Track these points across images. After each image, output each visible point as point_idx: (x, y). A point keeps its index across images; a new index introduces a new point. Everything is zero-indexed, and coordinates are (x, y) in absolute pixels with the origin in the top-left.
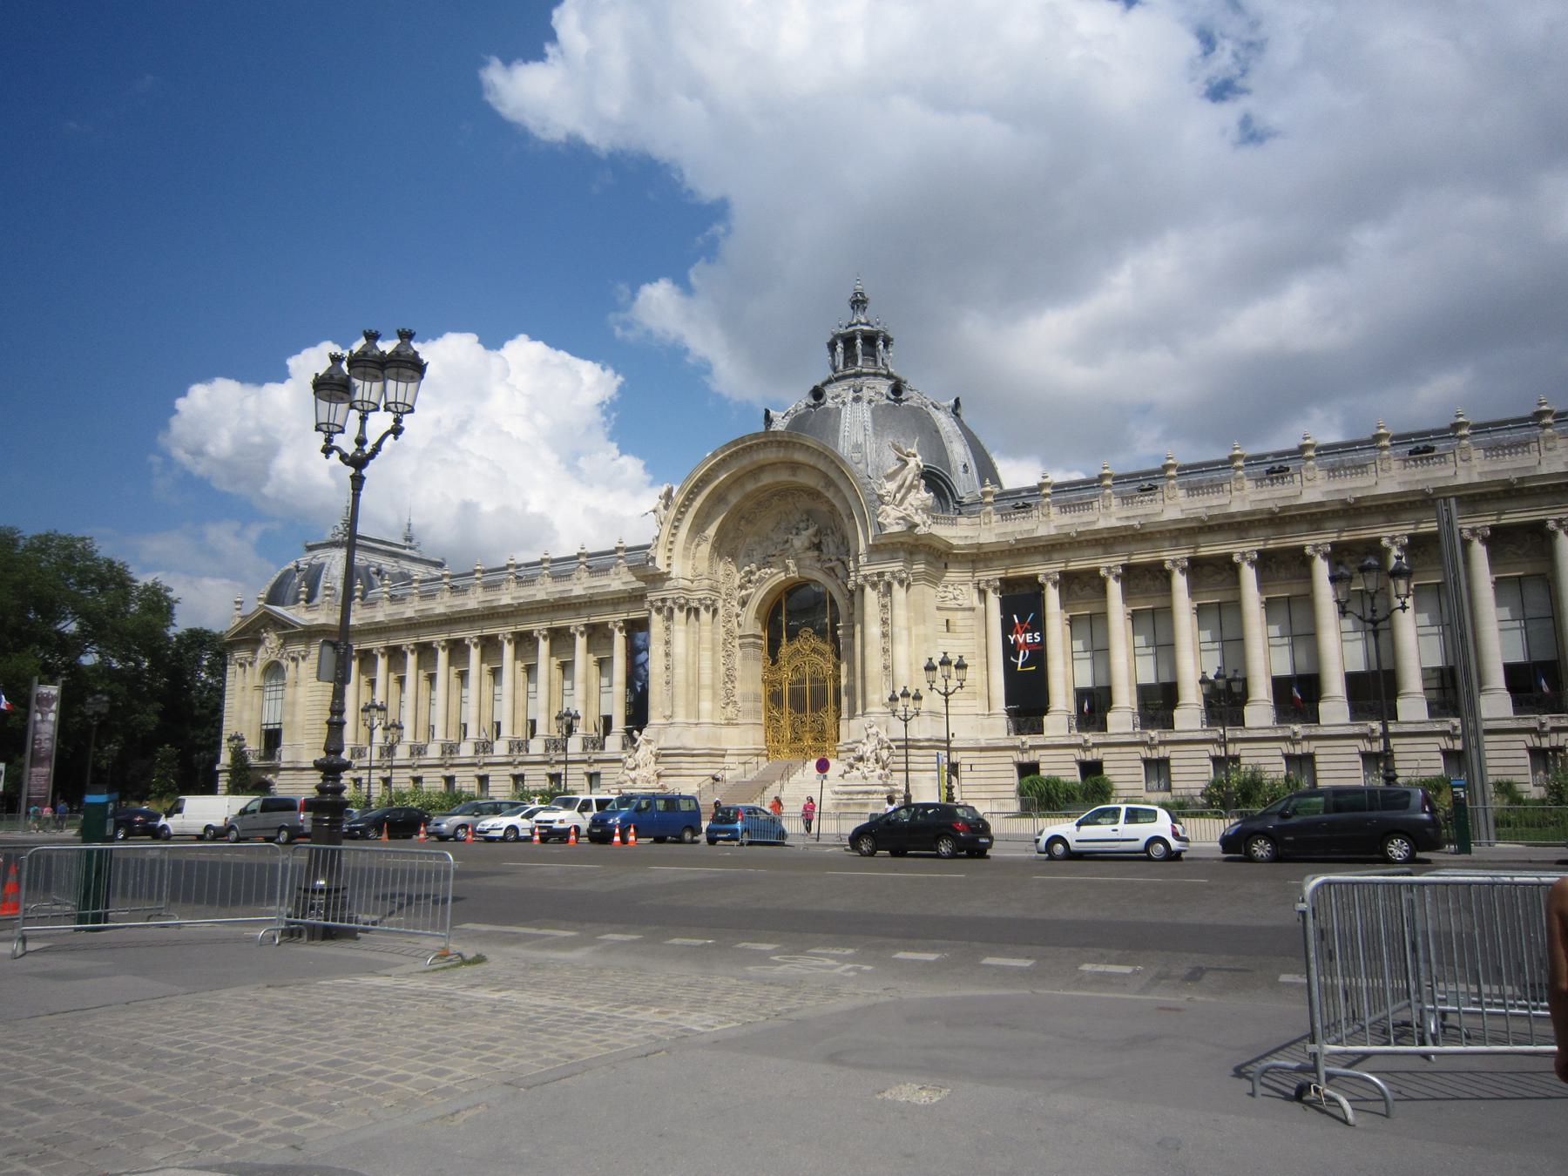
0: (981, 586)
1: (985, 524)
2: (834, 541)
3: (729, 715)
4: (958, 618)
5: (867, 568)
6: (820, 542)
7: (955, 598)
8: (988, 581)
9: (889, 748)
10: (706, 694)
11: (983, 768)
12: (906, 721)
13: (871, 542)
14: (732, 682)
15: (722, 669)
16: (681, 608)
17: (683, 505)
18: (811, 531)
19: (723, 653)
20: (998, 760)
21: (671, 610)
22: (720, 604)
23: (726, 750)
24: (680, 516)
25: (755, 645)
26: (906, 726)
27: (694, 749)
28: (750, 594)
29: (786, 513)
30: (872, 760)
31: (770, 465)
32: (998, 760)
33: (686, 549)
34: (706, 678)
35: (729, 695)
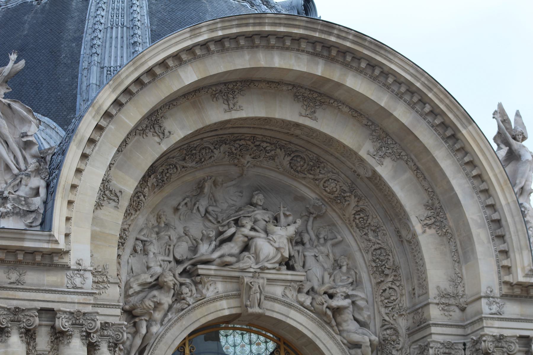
2: (316, 256)
5: (497, 324)
6: (293, 256)
13: (521, 279)
18: (291, 230)
31: (269, 82)
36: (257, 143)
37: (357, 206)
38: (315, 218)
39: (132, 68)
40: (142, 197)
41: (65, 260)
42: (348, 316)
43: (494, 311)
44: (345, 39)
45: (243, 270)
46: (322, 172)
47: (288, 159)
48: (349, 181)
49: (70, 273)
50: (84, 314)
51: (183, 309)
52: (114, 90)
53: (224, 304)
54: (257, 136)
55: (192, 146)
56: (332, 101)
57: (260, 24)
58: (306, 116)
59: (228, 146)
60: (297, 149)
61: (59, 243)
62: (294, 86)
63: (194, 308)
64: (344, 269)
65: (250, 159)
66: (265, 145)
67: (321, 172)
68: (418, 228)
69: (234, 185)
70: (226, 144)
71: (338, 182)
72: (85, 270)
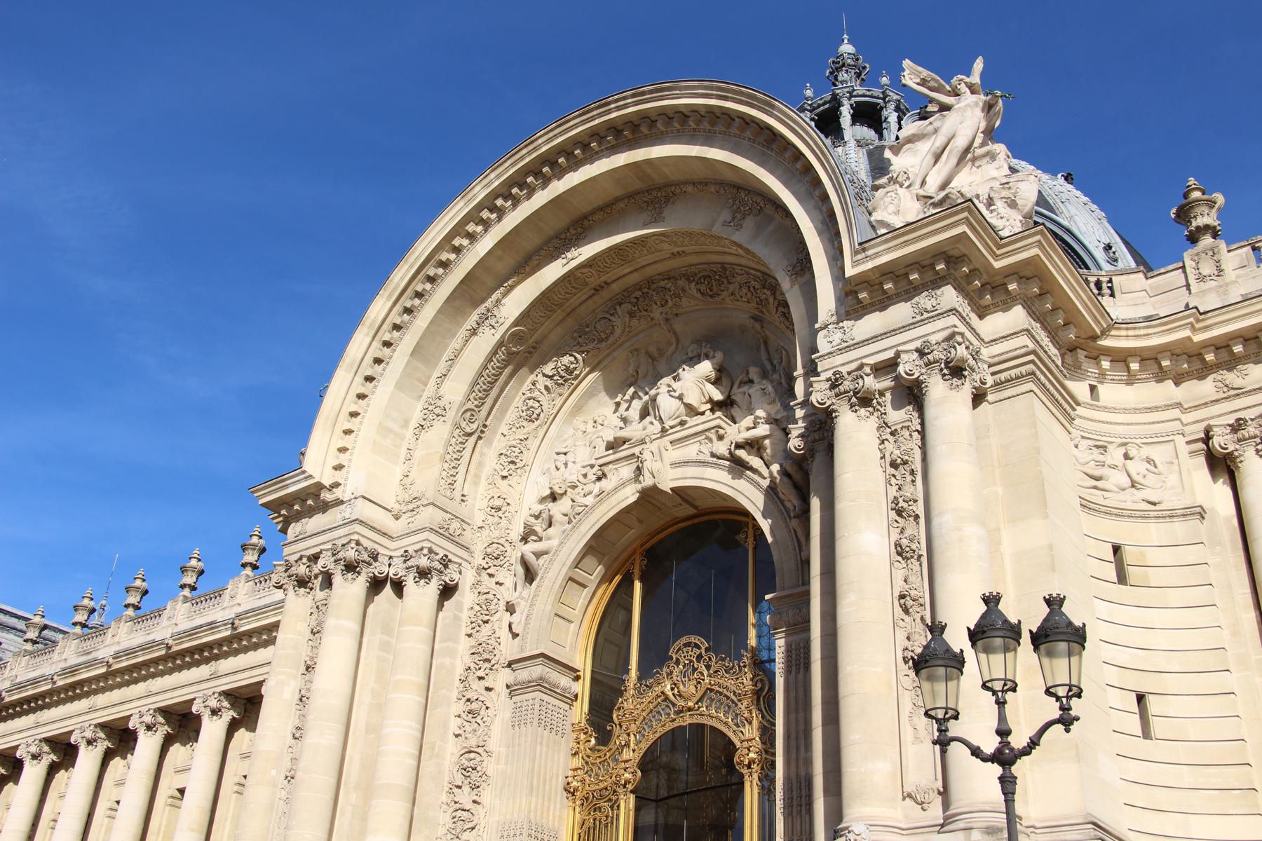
1: (1201, 278)
14: (475, 787)
19: (461, 707)
22: (467, 579)
31: (601, 209)
36: (655, 286)
37: (775, 299)
38: (766, 343)
39: (406, 267)
40: (531, 403)
41: (338, 493)
43: (834, 344)
44: (625, 107)
46: (734, 280)
47: (693, 285)
48: (758, 274)
49: (342, 507)
50: (343, 545)
51: (579, 514)
54: (653, 278)
55: (585, 324)
56: (673, 189)
57: (535, 149)
59: (623, 306)
60: (700, 269)
61: (314, 478)
62: (631, 196)
65: (661, 309)
66: (663, 283)
67: (731, 281)
69: (677, 348)
70: (620, 304)
71: (750, 282)
72: (356, 498)
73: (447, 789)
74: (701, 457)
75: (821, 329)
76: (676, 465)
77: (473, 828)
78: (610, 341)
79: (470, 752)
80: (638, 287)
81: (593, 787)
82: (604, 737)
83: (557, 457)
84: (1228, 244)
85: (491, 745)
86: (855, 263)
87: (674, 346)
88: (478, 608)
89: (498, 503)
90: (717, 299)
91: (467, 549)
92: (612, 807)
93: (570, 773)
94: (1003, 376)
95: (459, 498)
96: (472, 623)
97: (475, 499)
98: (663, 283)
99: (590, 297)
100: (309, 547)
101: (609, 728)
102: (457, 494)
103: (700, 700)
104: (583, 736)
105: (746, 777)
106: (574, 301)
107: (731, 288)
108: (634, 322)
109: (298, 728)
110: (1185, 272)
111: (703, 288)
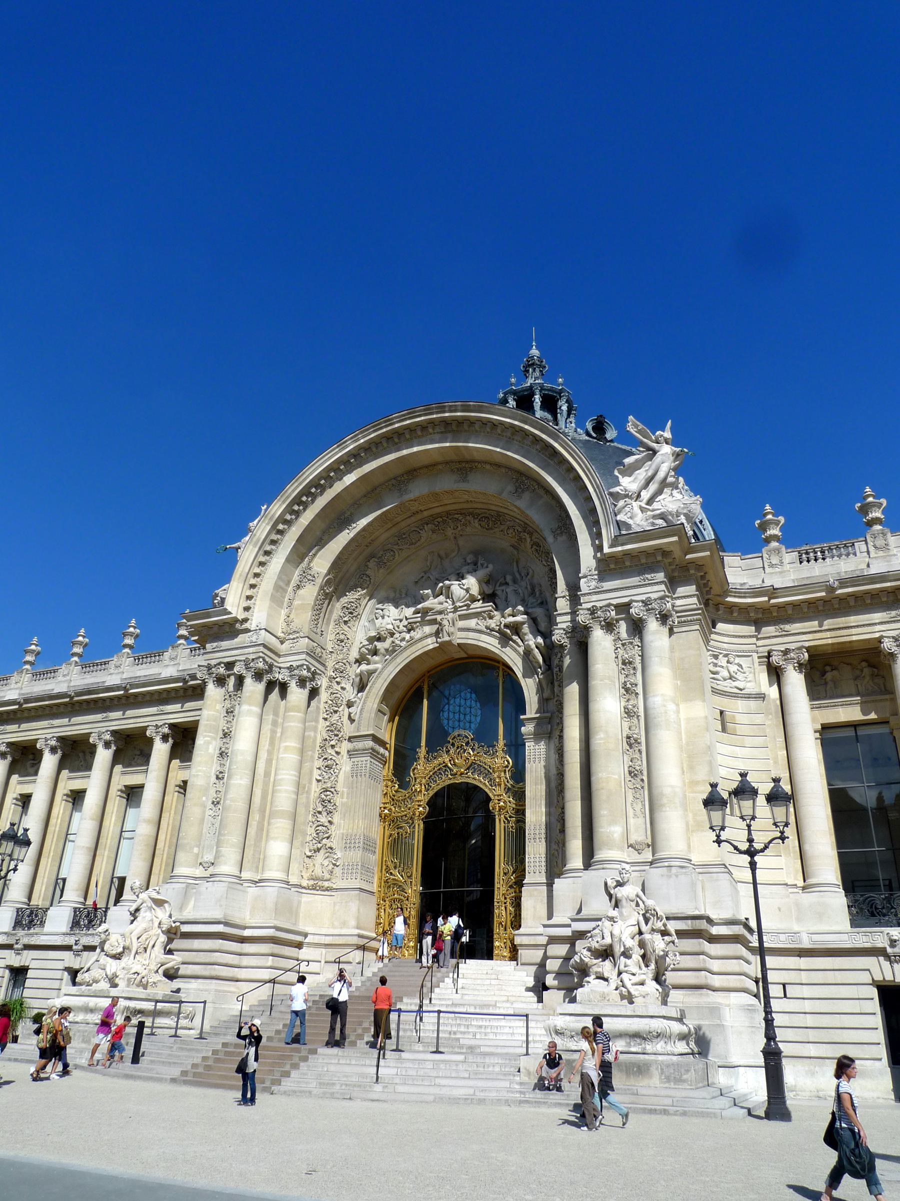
0: (776, 659)
1: (772, 566)
3: (318, 872)
4: (738, 708)
5: (594, 597)
7: (731, 677)
8: (786, 652)
9: (664, 933)
10: (281, 826)
11: (806, 992)
12: (751, 853)
14: (329, 813)
15: (315, 789)
16: (258, 676)
17: (281, 520)
19: (319, 763)
20: (839, 977)
21: (240, 680)
22: (323, 682)
23: (306, 935)
24: (274, 537)
25: (374, 753)
26: (753, 866)
27: (245, 928)
28: (374, 671)
29: (439, 556)
30: (636, 955)
31: (427, 467)
32: (839, 977)
33: (279, 589)
34: (284, 799)
35: (322, 834)
36: (450, 517)
38: (517, 562)
40: (364, 578)
42: (526, 629)
43: (591, 588)
45: (440, 613)
46: (504, 523)
47: (476, 521)
48: (522, 523)
52: (284, 502)
53: (430, 640)
56: (476, 464)
58: (459, 482)
63: (406, 648)
64: (538, 593)
65: (453, 531)
66: (457, 516)
68: (550, 539)
73: (312, 813)
74: (479, 627)
75: (583, 577)
76: (461, 630)
77: (328, 838)
78: (417, 544)
79: (327, 791)
80: (439, 515)
81: (397, 815)
82: (404, 785)
83: (377, 611)
84: (786, 548)
85: (339, 787)
86: (611, 546)
87: (456, 552)
88: (331, 702)
89: (342, 637)
90: (492, 532)
91: (324, 665)
92: (409, 827)
93: (382, 805)
94: (683, 619)
95: (320, 633)
96: (326, 711)
97: (327, 633)
98: (457, 516)
99: (409, 517)
100: (227, 657)
101: (408, 780)
102: (319, 631)
103: (468, 769)
104: (390, 783)
105: (497, 817)
106: (399, 519)
107: (502, 527)
108: (434, 536)
109: (221, 772)
110: (762, 559)
111: (483, 524)
